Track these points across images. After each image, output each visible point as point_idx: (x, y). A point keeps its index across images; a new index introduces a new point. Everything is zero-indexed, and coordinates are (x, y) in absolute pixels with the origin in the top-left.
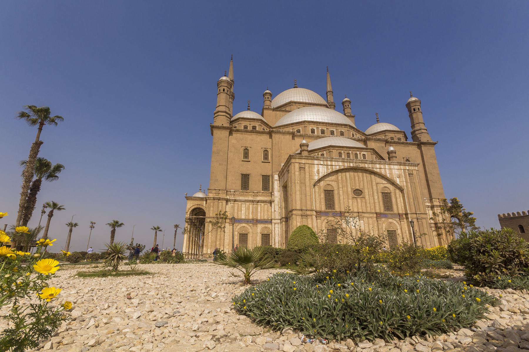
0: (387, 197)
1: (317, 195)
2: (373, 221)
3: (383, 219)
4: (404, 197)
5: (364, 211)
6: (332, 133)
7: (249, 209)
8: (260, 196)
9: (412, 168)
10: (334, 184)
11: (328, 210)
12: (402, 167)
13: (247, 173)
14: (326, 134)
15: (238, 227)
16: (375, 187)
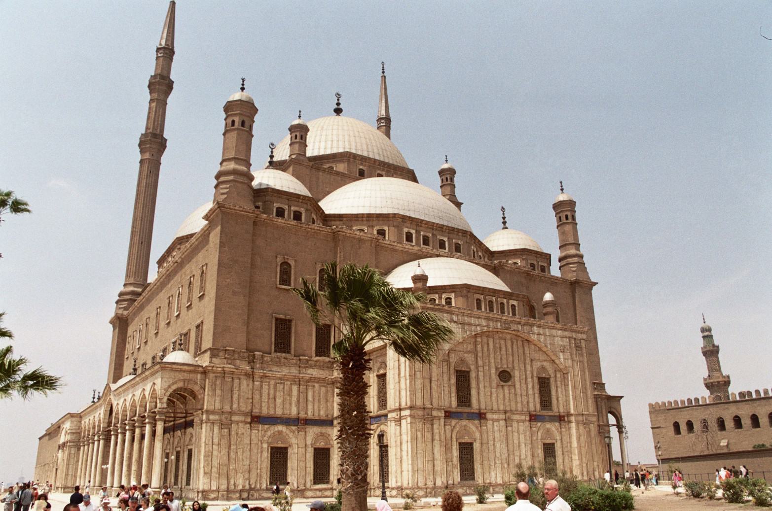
0: (544, 385)
1: (446, 379)
2: (524, 427)
3: (539, 424)
4: (566, 385)
5: (514, 409)
6: (442, 245)
7: (290, 395)
8: (311, 367)
9: (580, 336)
10: (469, 358)
11: (460, 409)
12: (567, 333)
13: (288, 317)
14: (431, 244)
15: (269, 433)
16: (528, 367)
